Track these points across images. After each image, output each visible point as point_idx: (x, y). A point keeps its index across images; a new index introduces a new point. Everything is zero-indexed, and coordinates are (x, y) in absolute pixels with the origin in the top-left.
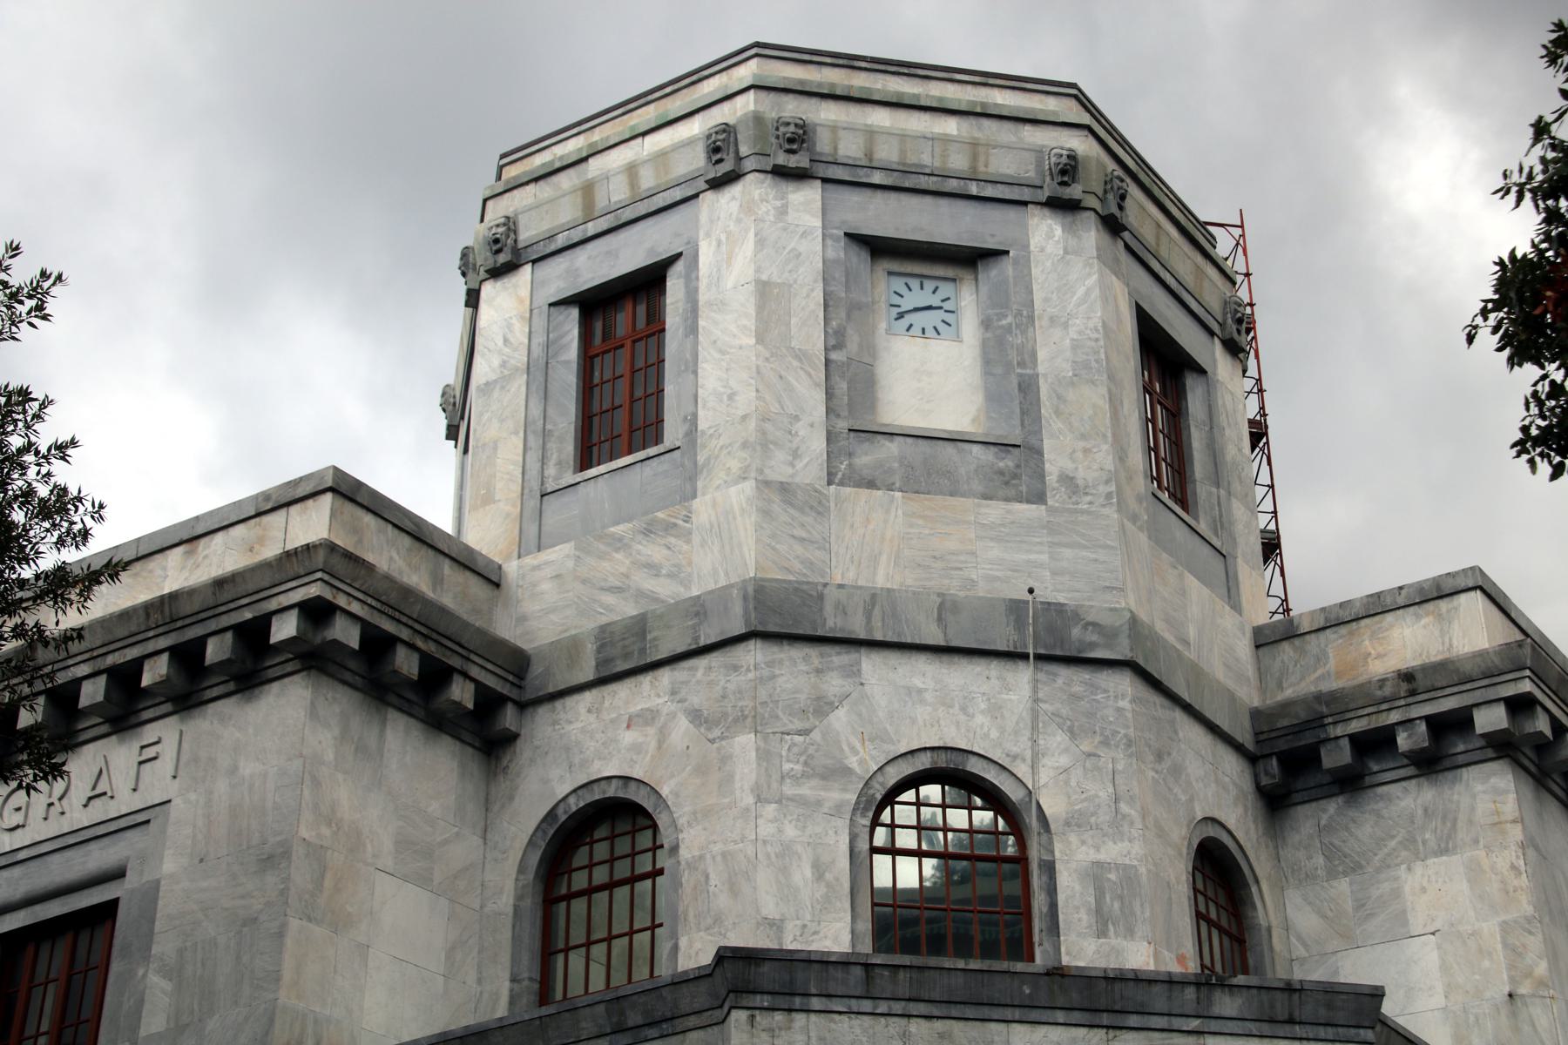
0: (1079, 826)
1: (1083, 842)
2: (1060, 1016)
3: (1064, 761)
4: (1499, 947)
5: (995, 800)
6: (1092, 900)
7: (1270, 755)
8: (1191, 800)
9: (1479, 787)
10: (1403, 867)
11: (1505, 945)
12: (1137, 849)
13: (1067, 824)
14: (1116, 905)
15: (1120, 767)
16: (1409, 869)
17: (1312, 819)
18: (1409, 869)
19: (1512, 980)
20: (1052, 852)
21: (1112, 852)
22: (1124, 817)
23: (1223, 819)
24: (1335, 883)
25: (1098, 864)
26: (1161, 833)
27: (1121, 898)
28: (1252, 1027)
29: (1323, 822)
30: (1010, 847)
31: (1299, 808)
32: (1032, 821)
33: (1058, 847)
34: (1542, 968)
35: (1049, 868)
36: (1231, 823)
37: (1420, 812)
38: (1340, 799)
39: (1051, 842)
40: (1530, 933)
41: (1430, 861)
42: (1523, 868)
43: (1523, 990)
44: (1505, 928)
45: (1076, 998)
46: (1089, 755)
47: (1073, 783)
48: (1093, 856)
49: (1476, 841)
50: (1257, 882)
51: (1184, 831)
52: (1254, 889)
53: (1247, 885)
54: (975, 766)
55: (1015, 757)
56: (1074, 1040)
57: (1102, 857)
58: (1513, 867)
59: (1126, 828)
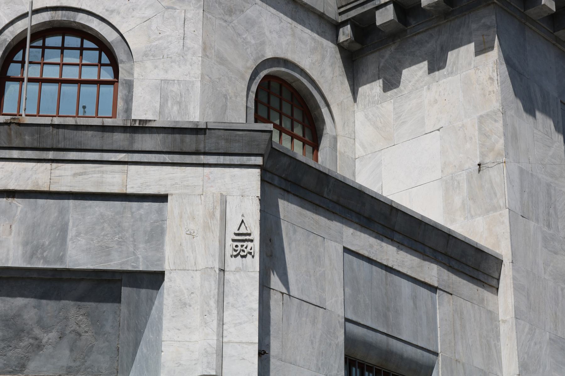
0: (154, 56)
1: (156, 67)
2: (15, 154)
3: (149, 13)
4: (477, 133)
5: (103, 46)
6: (158, 105)
7: (344, 23)
8: (263, 43)
9: (474, 26)
10: (426, 87)
11: (480, 129)
12: (197, 71)
13: (146, 55)
14: (175, 108)
15: (189, 15)
16: (429, 89)
17: (372, 61)
18: (429, 89)
19: (483, 155)
20: (133, 74)
21: (176, 72)
22: (189, 49)
23: (290, 56)
24: (385, 104)
25: (166, 81)
26: (222, 60)
27: (179, 103)
28: (167, 158)
29: (382, 64)
30: (107, 74)
31: (368, 57)
32: (120, 55)
33: (137, 71)
34: (500, 144)
35: (130, 85)
36: (305, 63)
37: (438, 49)
38: (393, 48)
39: (132, 69)
40: (496, 121)
41: (441, 82)
42: (495, 78)
43: (488, 160)
44: (481, 120)
45: (28, 140)
46: (168, 8)
47: (154, 27)
48: (162, 75)
49: (470, 64)
50: (328, 105)
51: (252, 65)
52: (324, 110)
53: (318, 107)
54: (82, 19)
55: (112, 11)
56: (25, 170)
57: (170, 76)
58: (491, 78)
59: (189, 56)
